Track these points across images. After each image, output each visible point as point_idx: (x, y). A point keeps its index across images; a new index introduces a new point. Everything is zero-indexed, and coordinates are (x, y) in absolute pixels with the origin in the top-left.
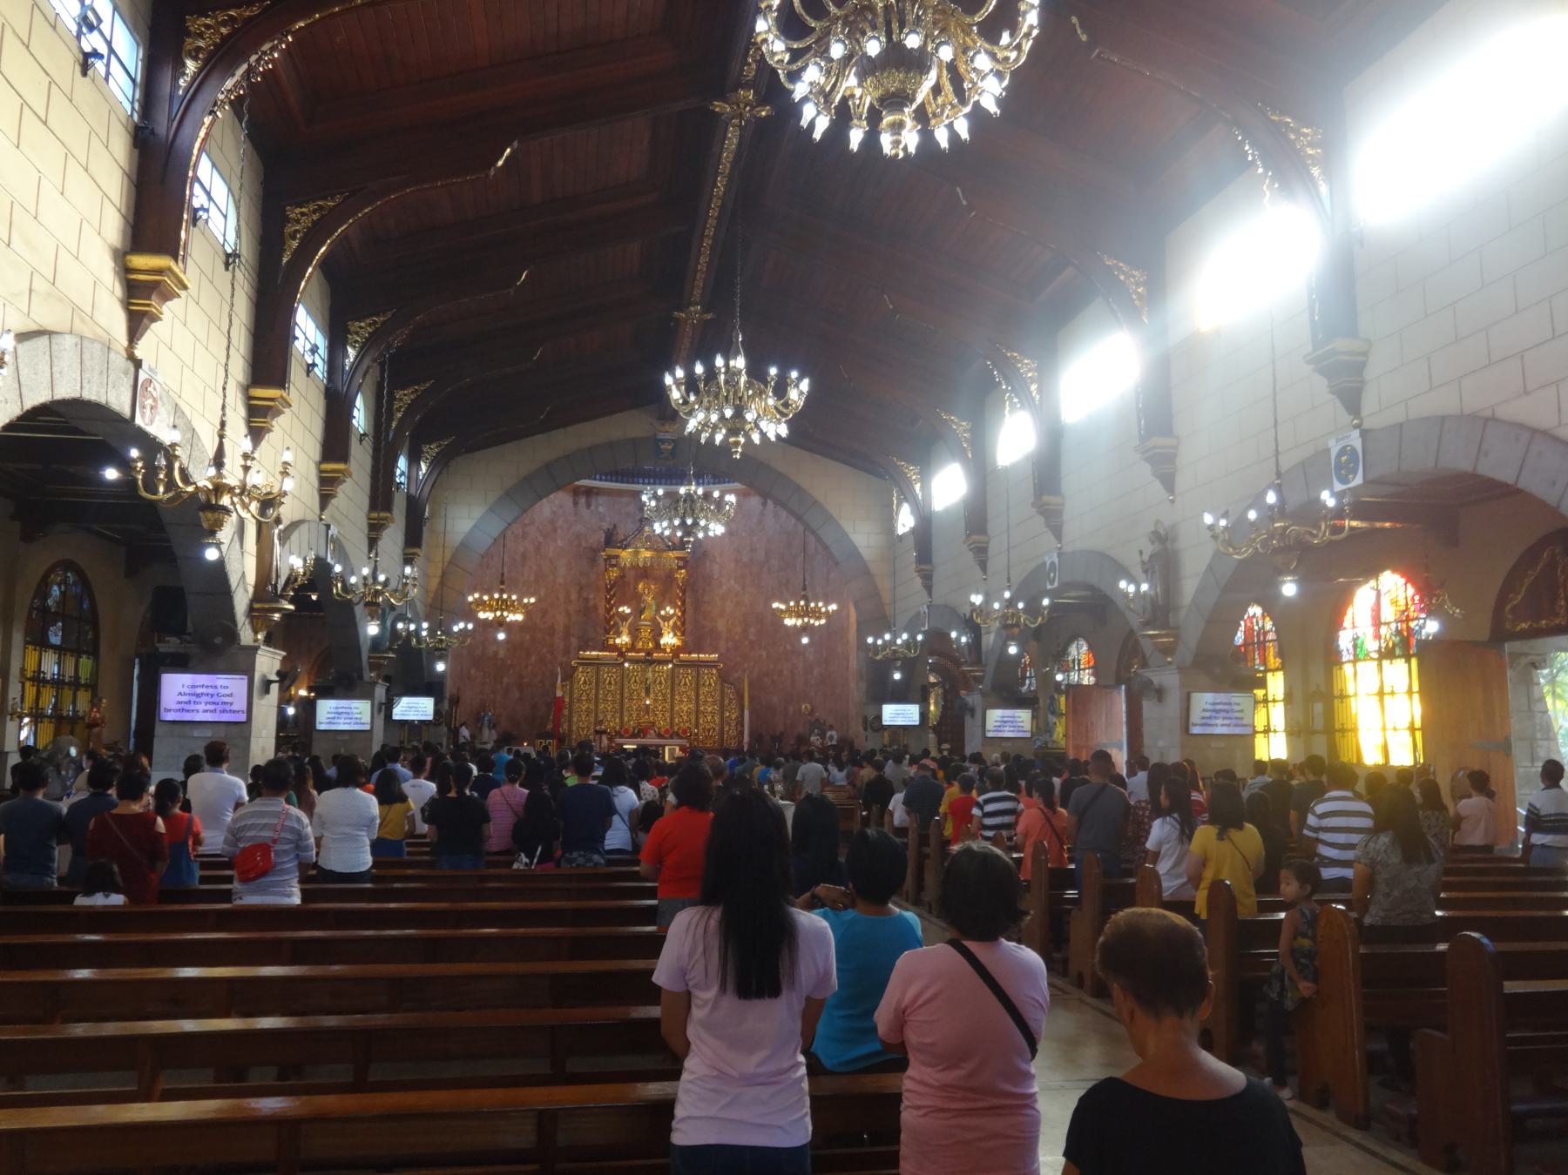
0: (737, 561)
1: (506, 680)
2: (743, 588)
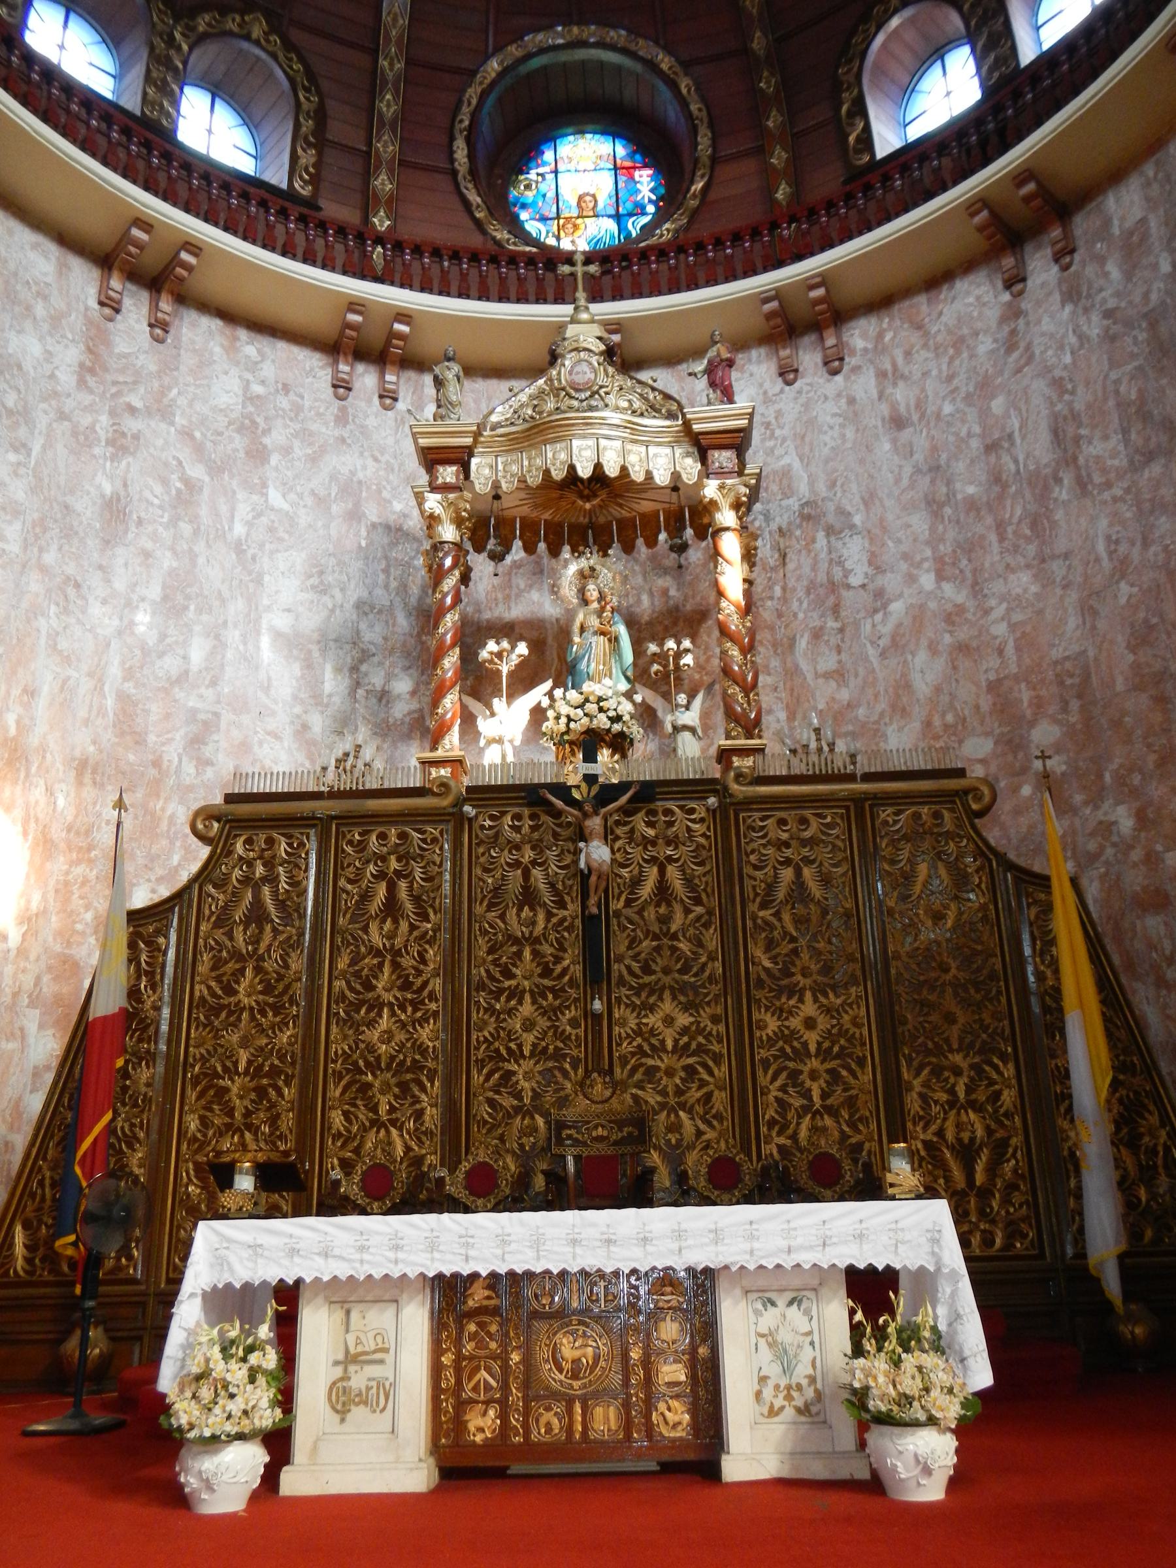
0: (934, 506)
2: (976, 589)
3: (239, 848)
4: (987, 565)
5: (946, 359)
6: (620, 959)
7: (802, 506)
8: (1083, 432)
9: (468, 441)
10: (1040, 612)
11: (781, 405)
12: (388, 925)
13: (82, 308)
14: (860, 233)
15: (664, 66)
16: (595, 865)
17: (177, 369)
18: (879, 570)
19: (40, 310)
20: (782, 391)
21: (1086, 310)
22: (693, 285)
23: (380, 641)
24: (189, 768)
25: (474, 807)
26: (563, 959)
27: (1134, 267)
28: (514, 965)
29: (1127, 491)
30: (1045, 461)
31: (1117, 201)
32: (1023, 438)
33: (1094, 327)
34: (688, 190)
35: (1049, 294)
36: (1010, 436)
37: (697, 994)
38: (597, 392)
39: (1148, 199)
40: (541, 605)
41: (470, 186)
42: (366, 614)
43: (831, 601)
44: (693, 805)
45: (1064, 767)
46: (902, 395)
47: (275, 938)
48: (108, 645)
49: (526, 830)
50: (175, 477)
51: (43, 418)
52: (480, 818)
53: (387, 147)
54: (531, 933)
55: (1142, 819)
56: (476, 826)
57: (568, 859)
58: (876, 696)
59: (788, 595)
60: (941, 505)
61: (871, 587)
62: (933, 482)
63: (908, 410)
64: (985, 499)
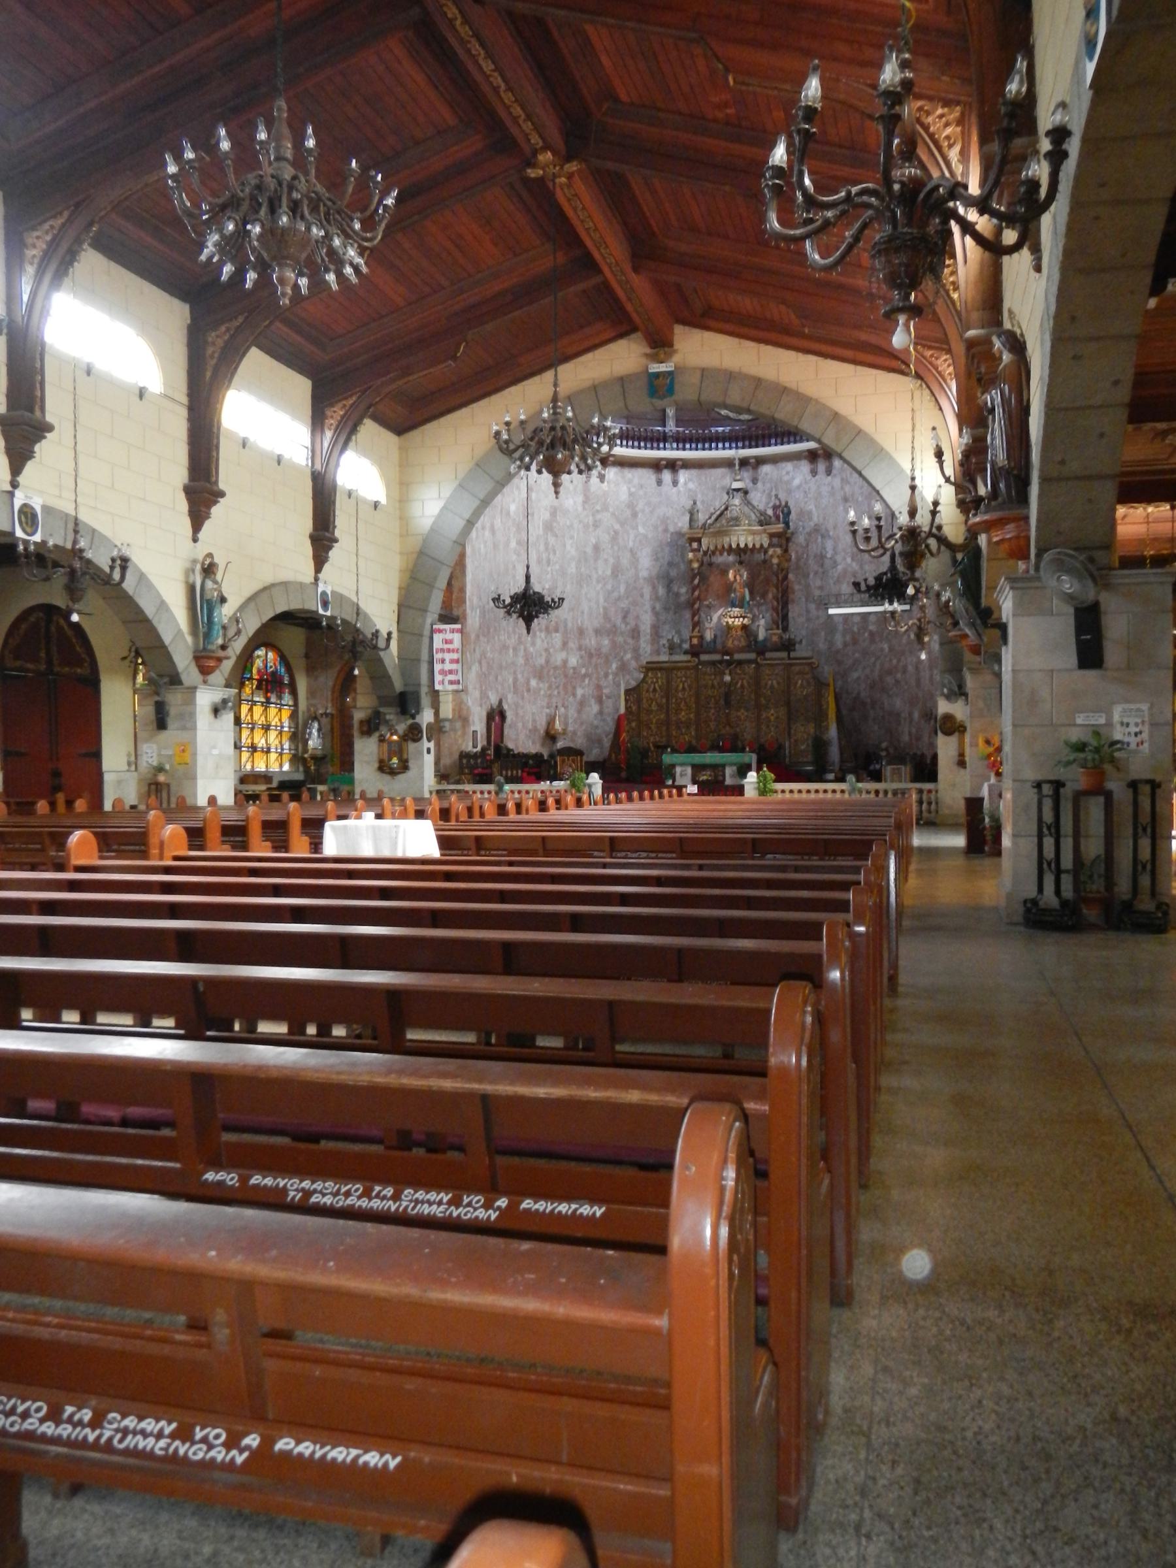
1: (579, 692)
24: (623, 626)
46: (847, 488)
51: (576, 526)
55: (891, 649)
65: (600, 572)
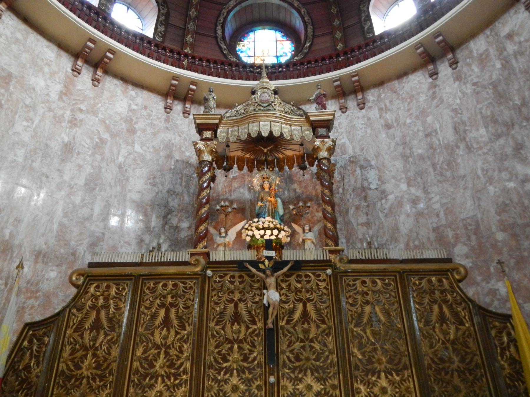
0: (405, 158)
2: (425, 190)
3: (92, 289)
4: (429, 180)
5: (407, 103)
6: (284, 352)
7: (350, 158)
8: (467, 128)
9: (217, 121)
10: (454, 199)
11: (340, 120)
12: (164, 332)
13: (65, 71)
14: (372, 57)
15: (296, 5)
16: (271, 302)
17: (102, 97)
18: (383, 182)
19: (46, 69)
20: (341, 115)
21: (465, 83)
22: (306, 75)
23: (176, 206)
25: (212, 271)
26: (254, 351)
27: (485, 66)
28: (229, 355)
29: (490, 150)
30: (451, 140)
31: (475, 44)
32: (441, 131)
33: (469, 89)
34: (304, 46)
35: (449, 78)
36: (436, 131)
37: (324, 373)
38: (271, 104)
39: (488, 42)
40: (244, 194)
41: (222, 42)
42: (172, 195)
43: (363, 194)
44: (319, 272)
45: (471, 265)
46: (389, 116)
47: (105, 338)
48: (57, 203)
49: (237, 283)
50: (96, 137)
51: (41, 109)
52: (214, 277)
53: (191, 26)
54: (238, 337)
56: (212, 280)
57: (257, 299)
58: (384, 233)
59: (345, 192)
60: (408, 157)
61: (380, 189)
62: (404, 148)
63: (392, 122)
64: (426, 155)
65: (67, 178)
